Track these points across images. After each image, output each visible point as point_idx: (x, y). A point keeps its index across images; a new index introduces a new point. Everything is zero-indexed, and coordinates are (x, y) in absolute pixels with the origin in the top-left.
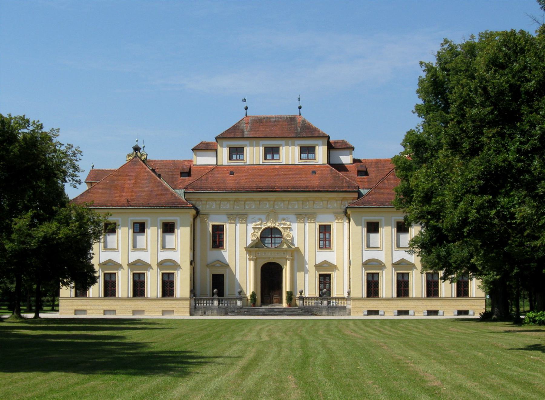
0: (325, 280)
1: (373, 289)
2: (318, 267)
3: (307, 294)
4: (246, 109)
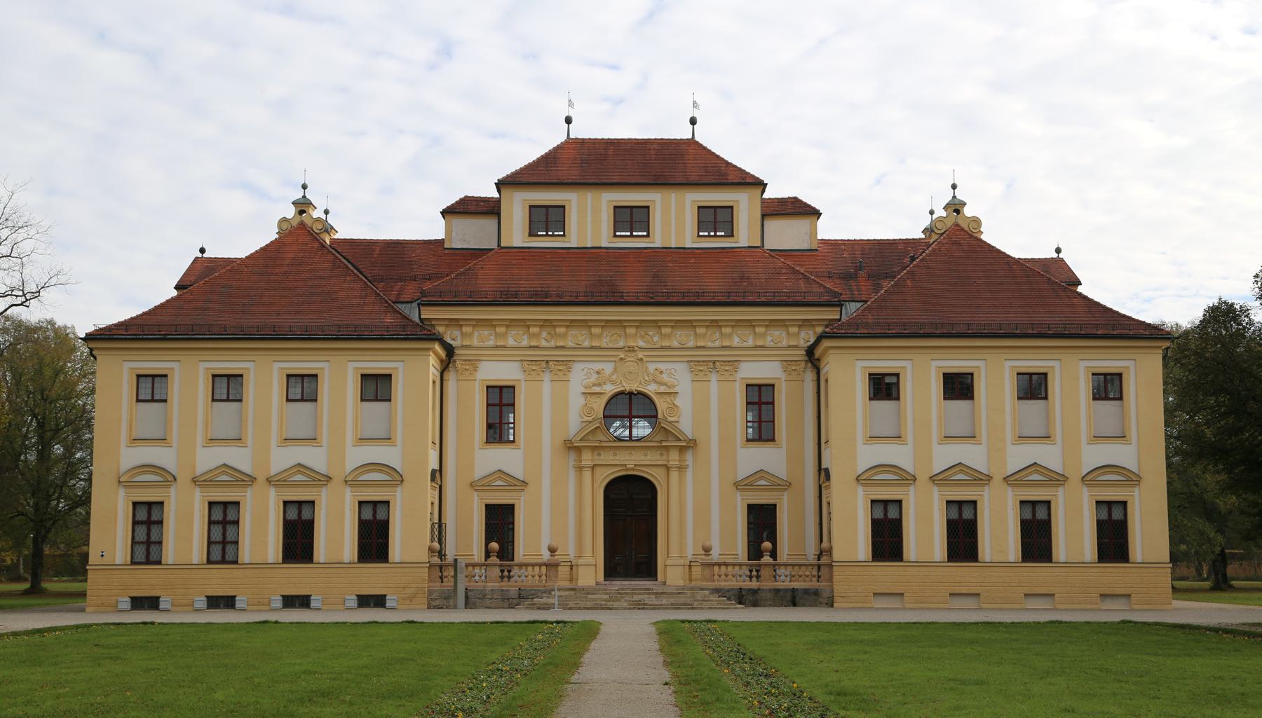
0: (762, 521)
1: (887, 538)
2: (743, 485)
3: (715, 555)
4: (568, 121)
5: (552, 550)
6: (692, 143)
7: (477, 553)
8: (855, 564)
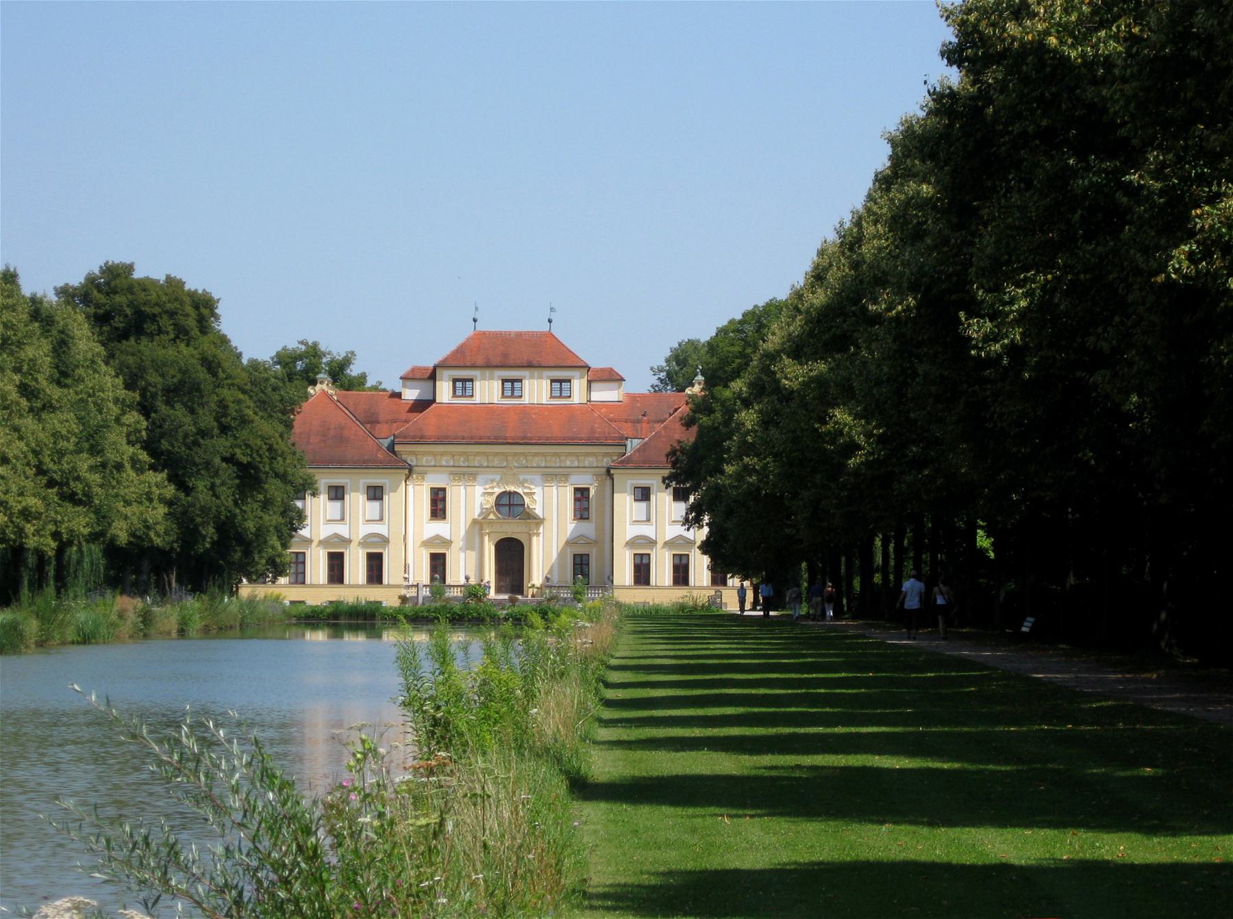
0: (581, 564)
1: (642, 574)
5: (467, 578)
6: (550, 335)
7: (425, 578)
8: (624, 587)
